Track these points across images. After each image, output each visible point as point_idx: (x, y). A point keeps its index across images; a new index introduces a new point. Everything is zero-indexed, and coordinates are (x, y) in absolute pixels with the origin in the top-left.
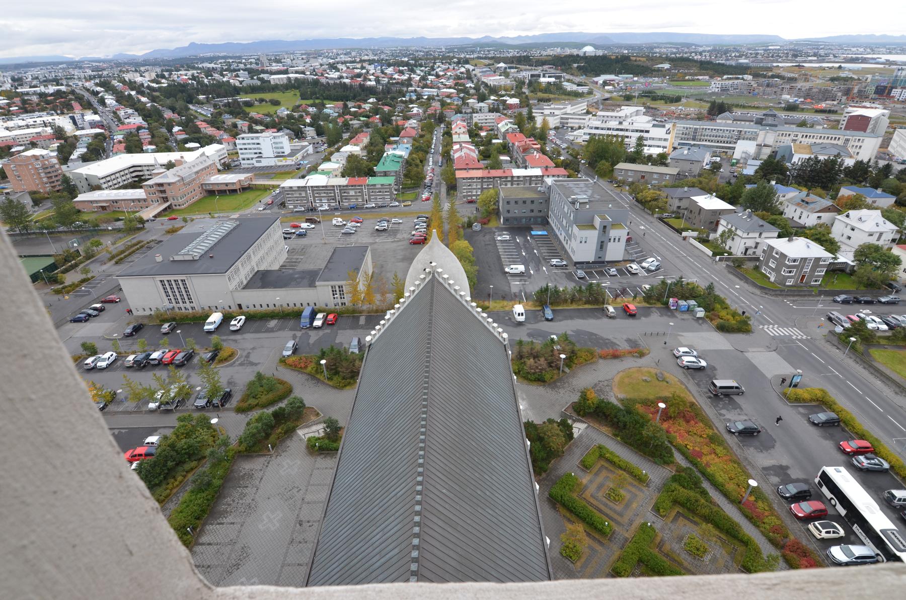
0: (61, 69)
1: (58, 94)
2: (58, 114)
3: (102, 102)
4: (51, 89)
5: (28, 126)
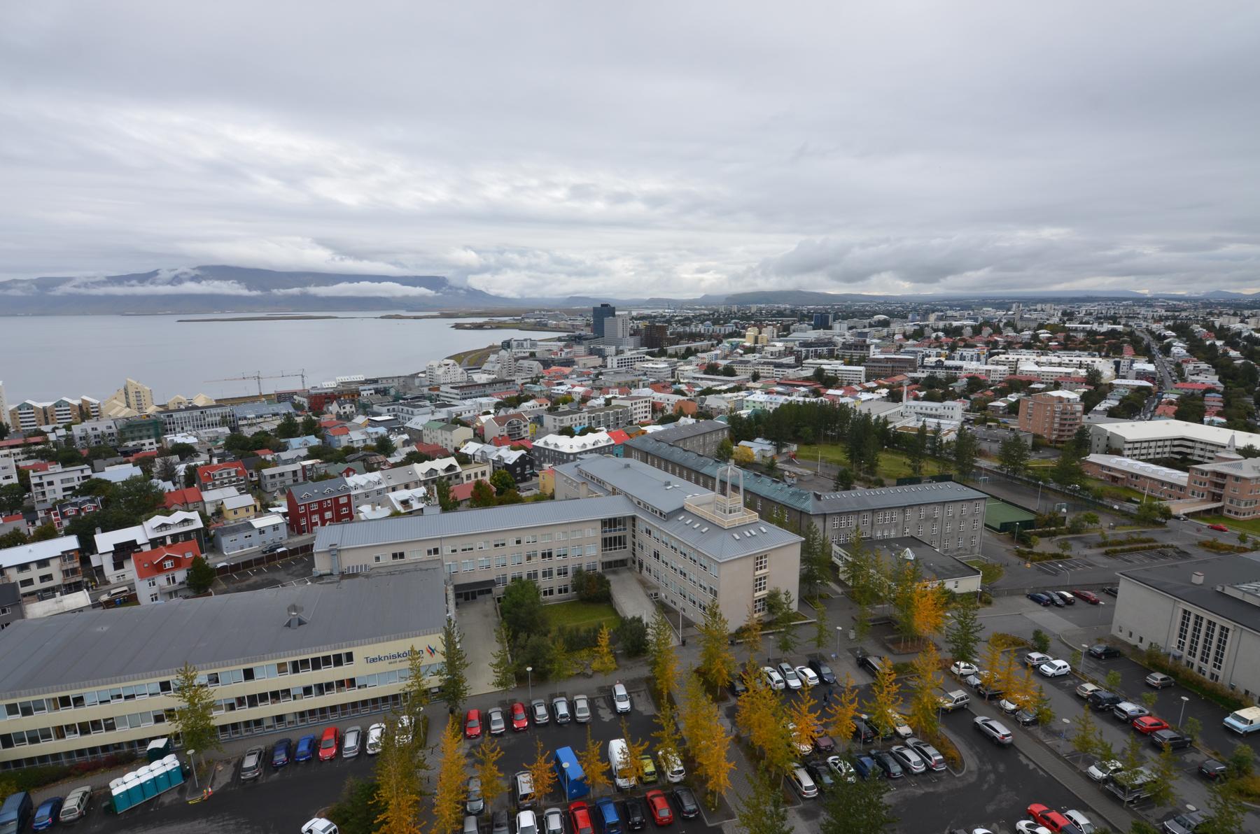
0: (1123, 305)
1: (1113, 333)
2: (1100, 357)
3: (1166, 350)
4: (1106, 327)
5: (1060, 365)
